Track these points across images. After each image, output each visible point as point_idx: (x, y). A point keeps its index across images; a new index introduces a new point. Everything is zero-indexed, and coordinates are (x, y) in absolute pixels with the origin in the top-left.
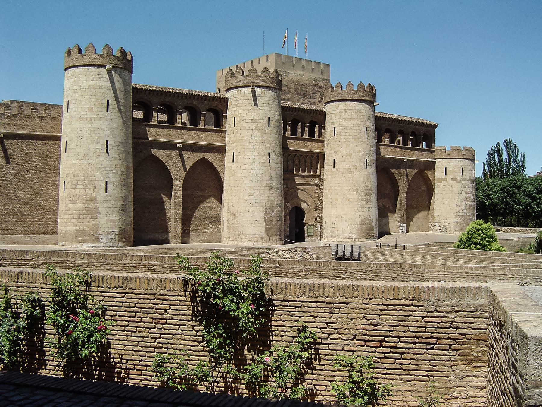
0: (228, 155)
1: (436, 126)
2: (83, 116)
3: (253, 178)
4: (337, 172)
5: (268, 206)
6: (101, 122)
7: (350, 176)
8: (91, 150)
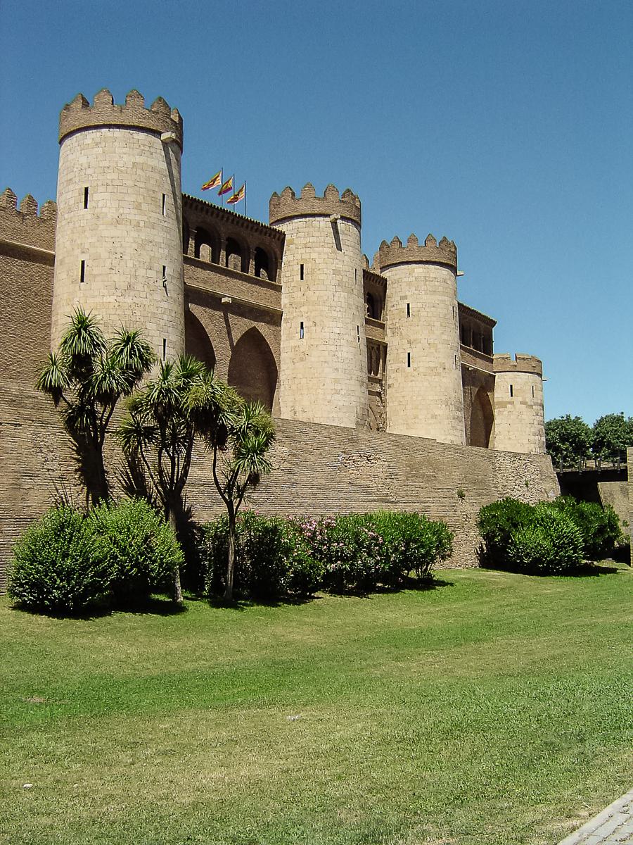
0: (288, 328)
1: (495, 323)
2: (123, 217)
3: (339, 365)
4: (416, 373)
5: (360, 412)
6: (155, 232)
7: (437, 380)
8: (139, 279)
